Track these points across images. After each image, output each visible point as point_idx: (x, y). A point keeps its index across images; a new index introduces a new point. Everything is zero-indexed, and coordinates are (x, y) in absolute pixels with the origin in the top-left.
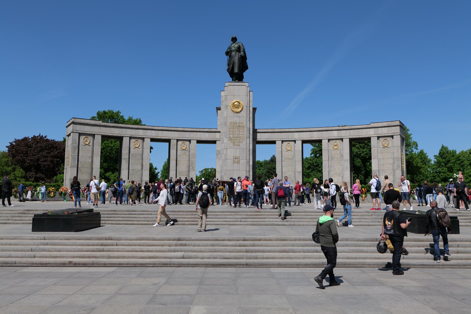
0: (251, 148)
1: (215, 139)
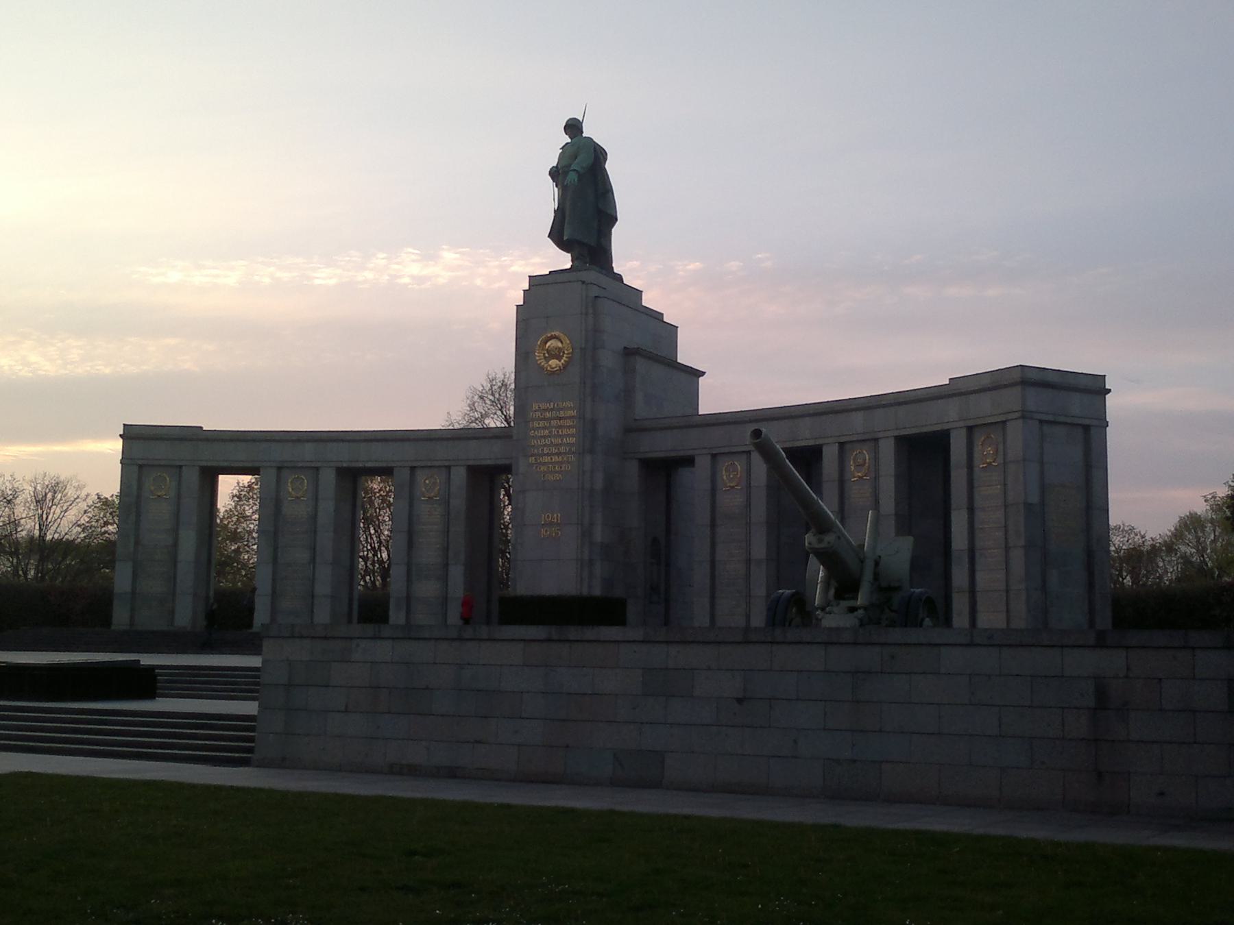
0: (599, 484)
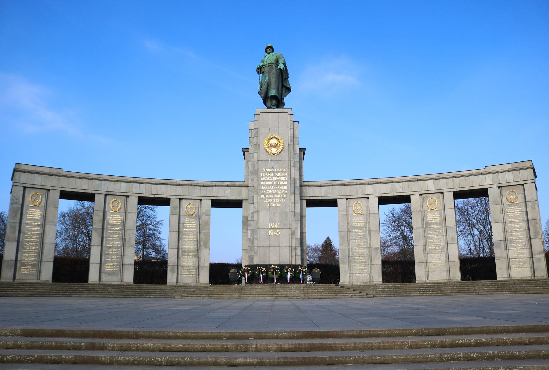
1: (241, 199)
